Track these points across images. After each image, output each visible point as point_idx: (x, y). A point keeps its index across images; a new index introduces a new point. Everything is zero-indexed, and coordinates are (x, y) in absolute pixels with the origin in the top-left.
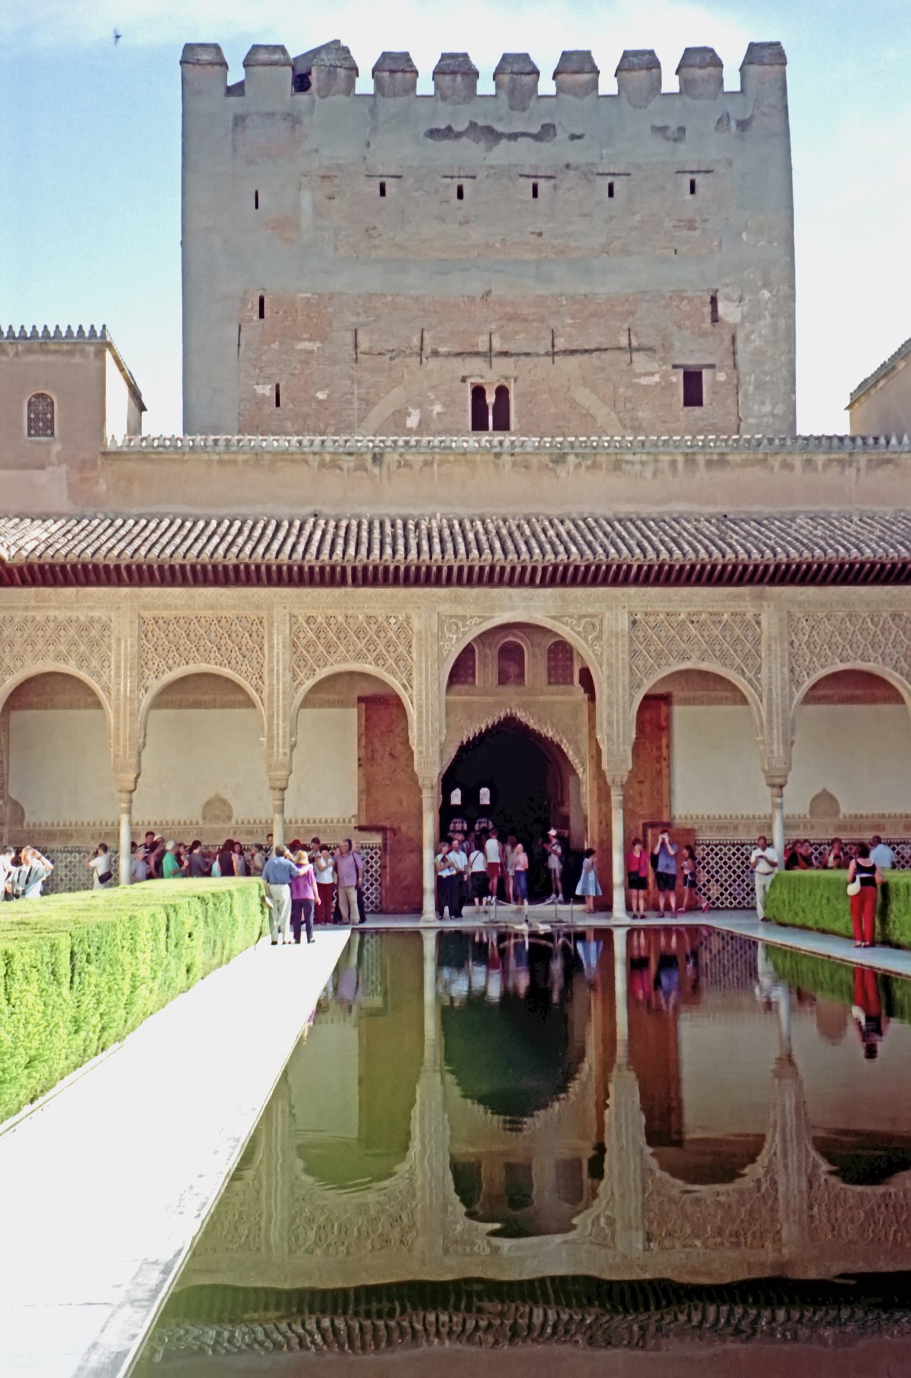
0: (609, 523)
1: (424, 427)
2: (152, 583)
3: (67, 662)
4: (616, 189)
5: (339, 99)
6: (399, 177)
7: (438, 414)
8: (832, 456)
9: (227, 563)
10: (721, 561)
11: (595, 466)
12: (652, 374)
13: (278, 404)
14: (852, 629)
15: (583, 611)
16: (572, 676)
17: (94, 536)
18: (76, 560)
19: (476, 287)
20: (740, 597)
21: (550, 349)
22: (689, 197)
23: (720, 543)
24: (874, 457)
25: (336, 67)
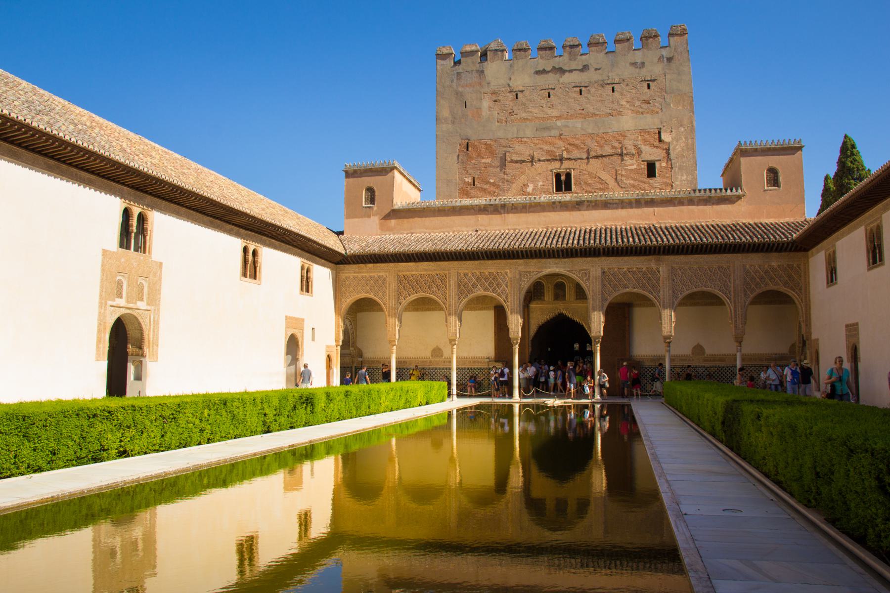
6: (522, 91)
7: (541, 185)
12: (632, 165)
13: (474, 185)
19: (554, 133)
22: (648, 90)
25: (496, 50)
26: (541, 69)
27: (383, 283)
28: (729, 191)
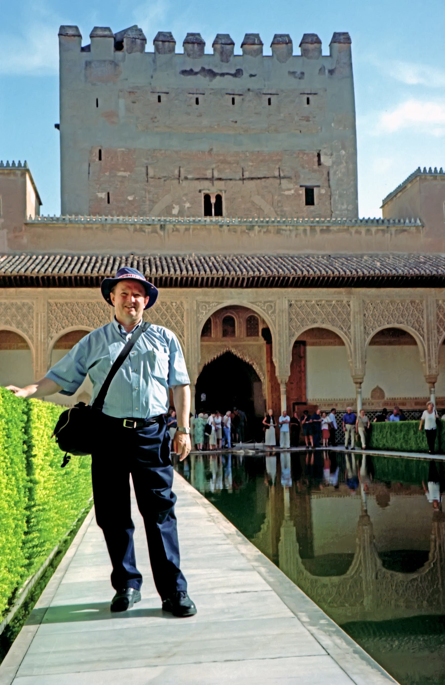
0: (276, 258)
1: (181, 213)
2: (54, 286)
3: (11, 325)
4: (272, 101)
5: (138, 55)
6: (167, 93)
7: (188, 208)
8: (380, 228)
9: (93, 275)
10: (332, 275)
11: (268, 231)
13: (109, 202)
14: (393, 308)
15: (266, 300)
16: (258, 332)
17: (23, 263)
18: (16, 274)
20: (340, 293)
21: (242, 177)
22: (306, 106)
23: (331, 267)
24: (399, 228)
25: (136, 39)
26: (188, 69)
27: (29, 312)
28: (407, 221)
